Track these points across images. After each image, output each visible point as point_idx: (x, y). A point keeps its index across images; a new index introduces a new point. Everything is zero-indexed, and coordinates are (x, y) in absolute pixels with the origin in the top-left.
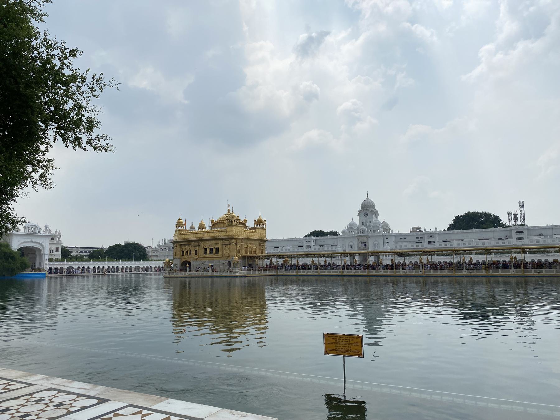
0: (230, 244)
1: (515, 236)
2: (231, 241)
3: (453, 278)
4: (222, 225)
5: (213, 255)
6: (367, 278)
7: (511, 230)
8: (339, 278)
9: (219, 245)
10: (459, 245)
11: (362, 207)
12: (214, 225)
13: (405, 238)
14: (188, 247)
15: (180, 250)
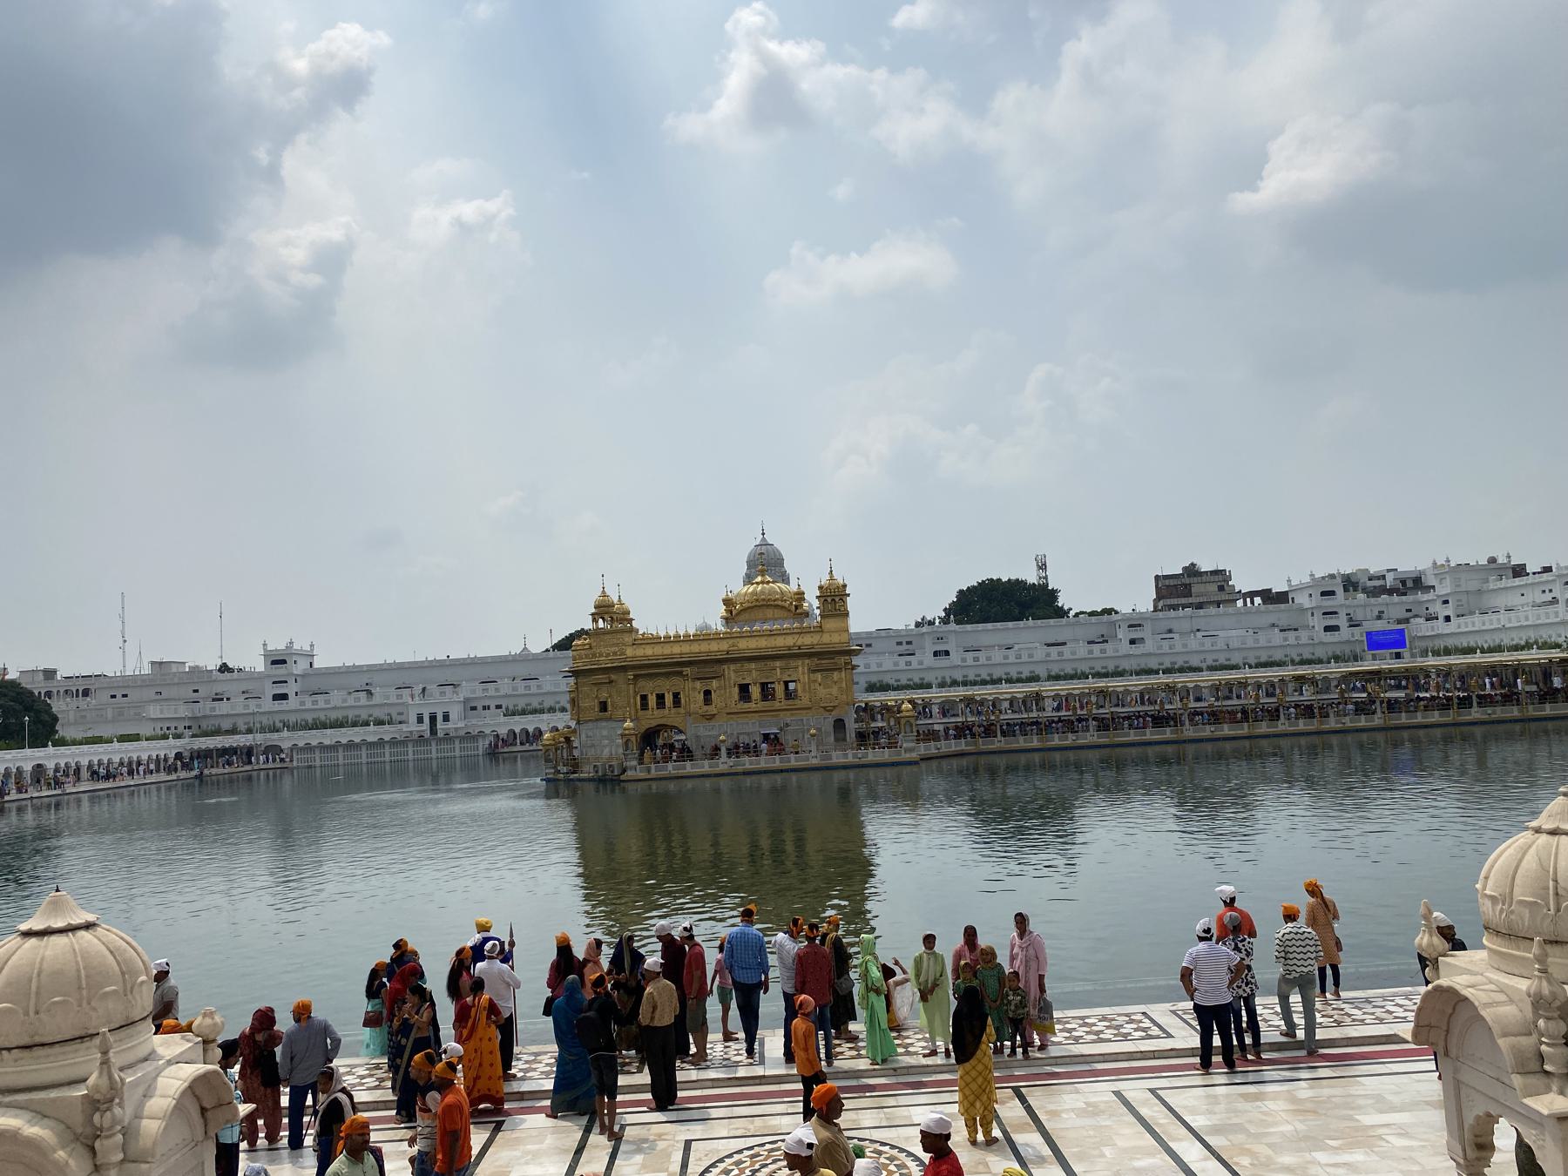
0: (840, 669)
1: (1124, 634)
2: (842, 660)
3: (1452, 729)
4: (770, 613)
5: (777, 705)
6: (1247, 743)
7: (1114, 623)
8: (1170, 749)
9: (800, 671)
10: (1006, 657)
11: (751, 564)
12: (735, 611)
13: (869, 645)
14: (667, 687)
15: (636, 693)
